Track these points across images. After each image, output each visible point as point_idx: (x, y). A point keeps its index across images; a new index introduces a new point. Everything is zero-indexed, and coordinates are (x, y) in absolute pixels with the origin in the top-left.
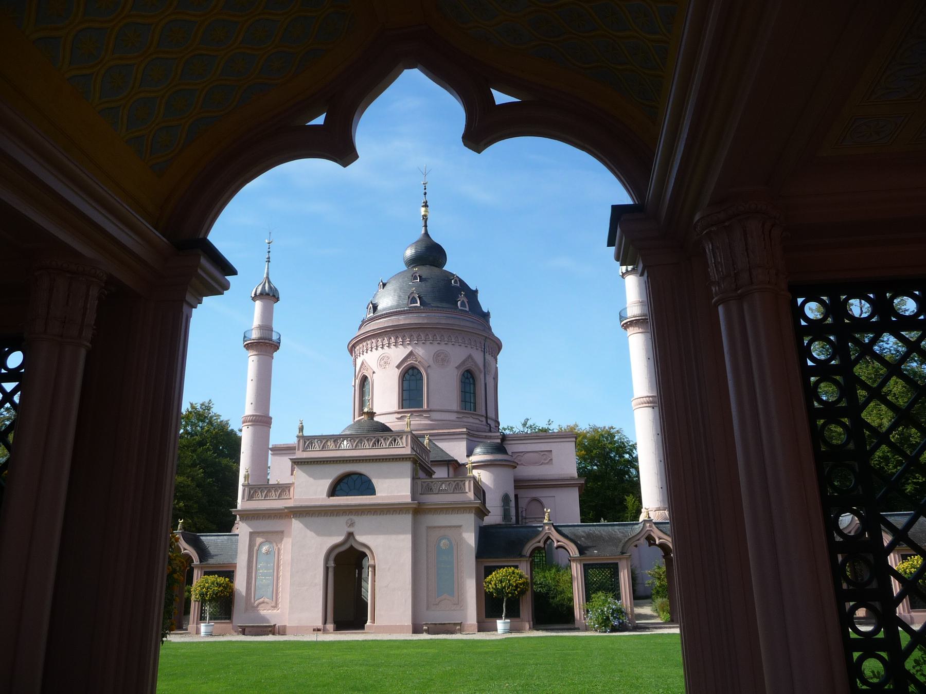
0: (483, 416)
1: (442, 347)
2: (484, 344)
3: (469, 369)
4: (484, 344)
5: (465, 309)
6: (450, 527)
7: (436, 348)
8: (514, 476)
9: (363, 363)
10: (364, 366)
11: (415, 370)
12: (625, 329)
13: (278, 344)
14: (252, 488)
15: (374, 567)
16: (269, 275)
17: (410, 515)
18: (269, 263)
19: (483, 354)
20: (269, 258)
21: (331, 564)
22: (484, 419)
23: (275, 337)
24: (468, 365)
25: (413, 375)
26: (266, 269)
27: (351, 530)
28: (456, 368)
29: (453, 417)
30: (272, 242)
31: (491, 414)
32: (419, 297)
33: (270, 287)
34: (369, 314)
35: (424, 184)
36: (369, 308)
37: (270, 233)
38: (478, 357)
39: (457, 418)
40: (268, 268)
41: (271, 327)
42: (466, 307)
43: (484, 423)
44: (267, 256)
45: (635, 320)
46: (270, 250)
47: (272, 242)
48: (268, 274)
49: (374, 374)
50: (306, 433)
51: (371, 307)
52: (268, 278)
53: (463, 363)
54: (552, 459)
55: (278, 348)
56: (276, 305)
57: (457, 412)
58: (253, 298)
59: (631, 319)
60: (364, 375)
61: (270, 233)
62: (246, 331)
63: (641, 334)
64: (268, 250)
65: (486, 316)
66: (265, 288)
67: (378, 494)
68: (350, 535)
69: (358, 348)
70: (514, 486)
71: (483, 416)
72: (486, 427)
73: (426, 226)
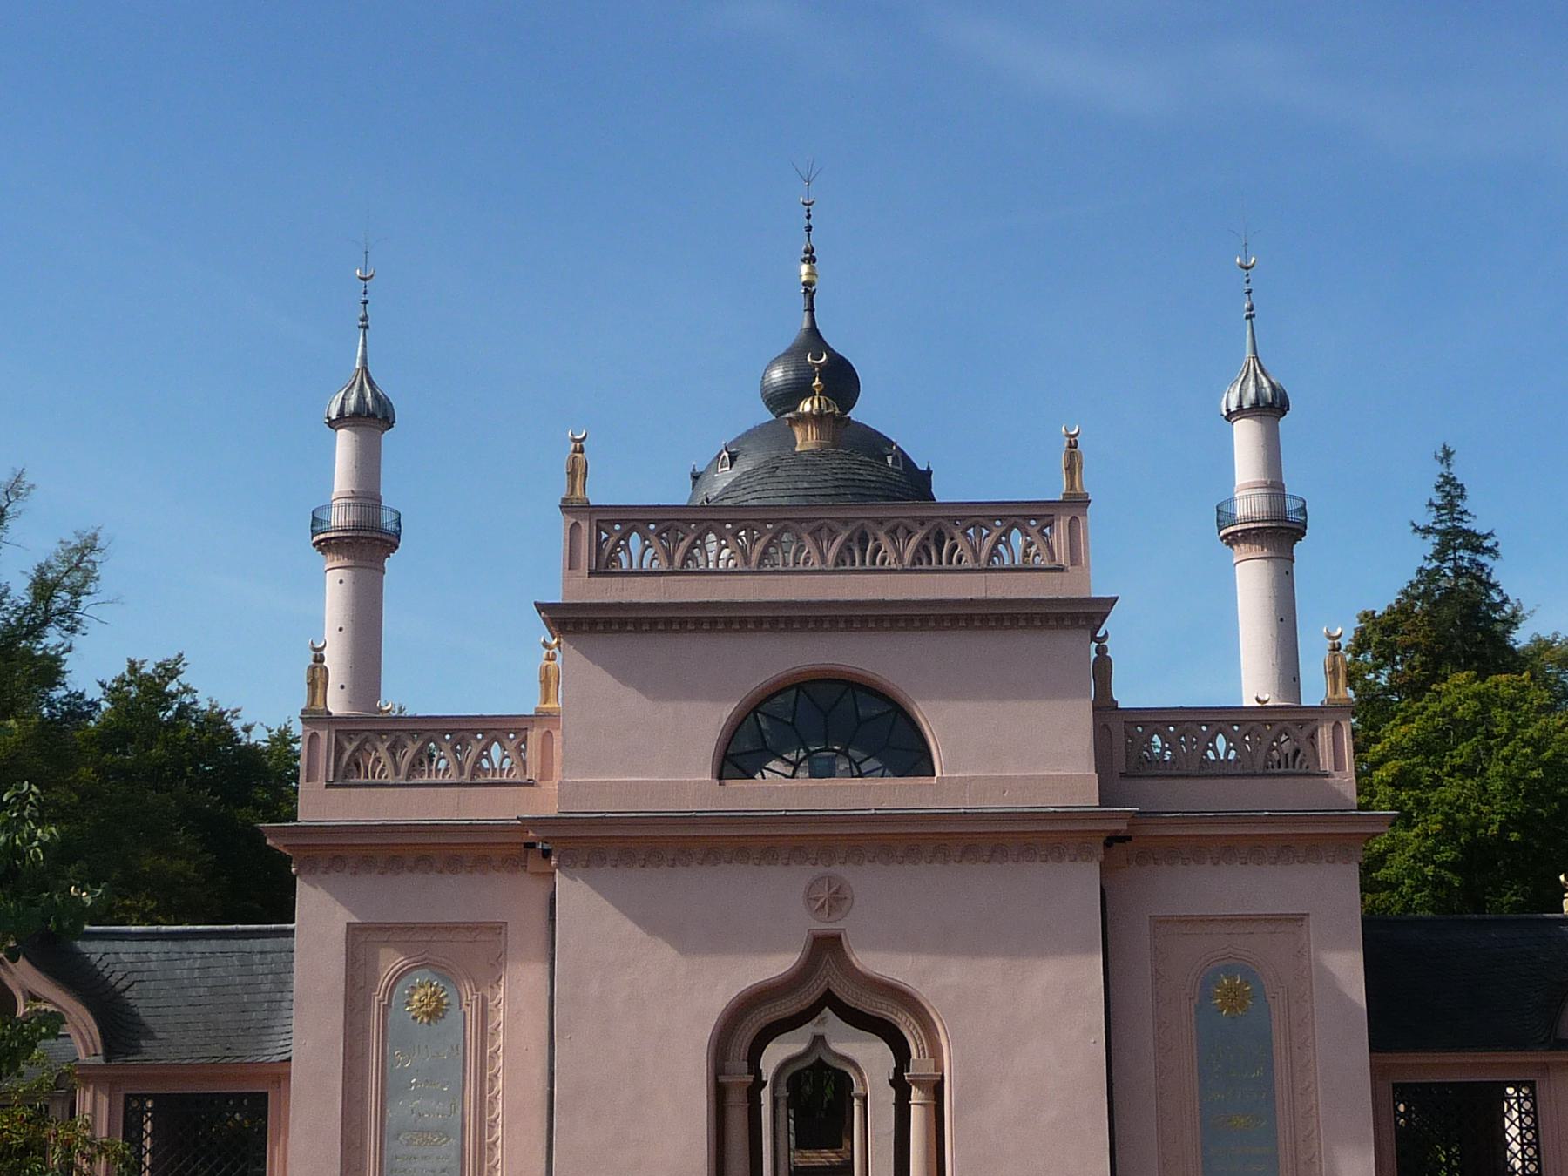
12: (1229, 544)
15: (865, 1099)
16: (369, 361)
18: (367, 331)
20: (365, 319)
26: (360, 348)
33: (376, 396)
37: (367, 252)
40: (364, 346)
44: (362, 314)
45: (1254, 529)
46: (367, 297)
48: (364, 359)
52: (365, 369)
59: (1245, 526)
61: (367, 252)
63: (1265, 561)
66: (364, 399)
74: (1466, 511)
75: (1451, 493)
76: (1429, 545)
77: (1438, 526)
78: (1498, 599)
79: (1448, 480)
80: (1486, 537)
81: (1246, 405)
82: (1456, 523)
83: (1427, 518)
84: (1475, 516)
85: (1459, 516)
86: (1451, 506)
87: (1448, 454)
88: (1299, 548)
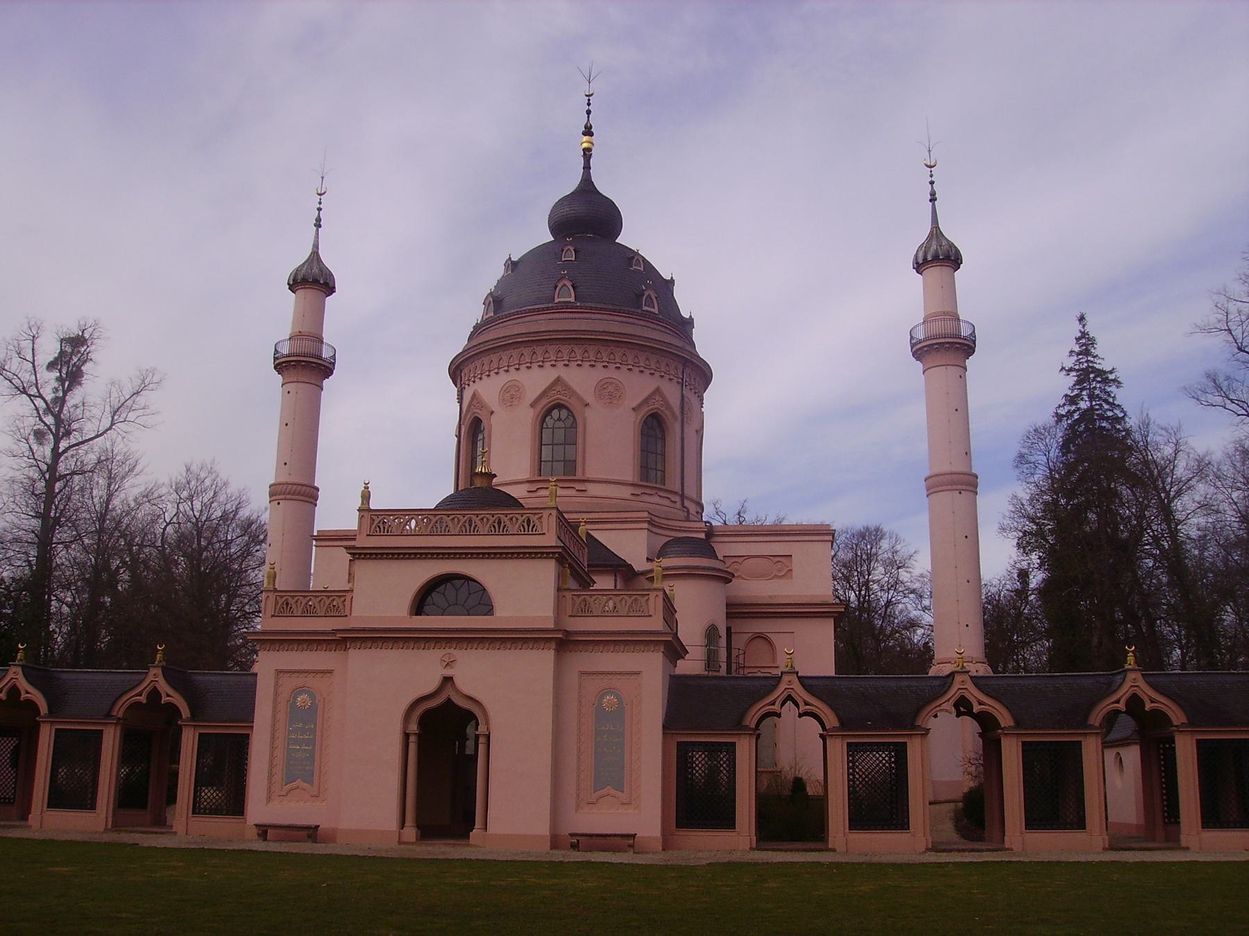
0: (676, 493)
1: (612, 373)
2: (683, 371)
3: (656, 412)
4: (683, 371)
5: (652, 310)
6: (620, 673)
7: (599, 374)
8: (727, 597)
9: (474, 396)
10: (475, 402)
11: (564, 413)
13: (331, 366)
14: (282, 597)
15: (488, 737)
17: (552, 652)
19: (679, 387)
21: (413, 727)
22: (677, 499)
23: (326, 354)
24: (656, 405)
25: (559, 419)
27: (448, 672)
28: (633, 409)
29: (626, 492)
30: (325, 193)
31: (690, 491)
32: (573, 286)
34: (487, 314)
35: (586, 96)
36: (487, 302)
37: (323, 178)
38: (672, 393)
39: (632, 494)
41: (322, 336)
42: (654, 307)
43: (678, 505)
45: (937, 344)
47: (325, 193)
48: (316, 246)
49: (492, 416)
50: (374, 505)
51: (490, 302)
53: (646, 401)
54: (792, 570)
55: (332, 373)
56: (329, 300)
57: (633, 485)
58: (292, 285)
60: (476, 417)
61: (323, 178)
62: (279, 342)
64: (318, 206)
65: (690, 322)
67: (499, 613)
68: (448, 680)
69: (466, 371)
70: (727, 613)
71: (676, 493)
72: (681, 512)
73: (587, 167)
74: (1097, 356)
75: (1086, 344)
76: (1072, 379)
77: (1077, 367)
78: (1121, 415)
79: (1084, 335)
80: (1111, 372)
81: (929, 258)
82: (1091, 365)
83: (1070, 362)
84: (1103, 359)
85: (1092, 359)
86: (1086, 352)
87: (1081, 319)
88: (969, 362)
